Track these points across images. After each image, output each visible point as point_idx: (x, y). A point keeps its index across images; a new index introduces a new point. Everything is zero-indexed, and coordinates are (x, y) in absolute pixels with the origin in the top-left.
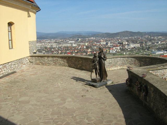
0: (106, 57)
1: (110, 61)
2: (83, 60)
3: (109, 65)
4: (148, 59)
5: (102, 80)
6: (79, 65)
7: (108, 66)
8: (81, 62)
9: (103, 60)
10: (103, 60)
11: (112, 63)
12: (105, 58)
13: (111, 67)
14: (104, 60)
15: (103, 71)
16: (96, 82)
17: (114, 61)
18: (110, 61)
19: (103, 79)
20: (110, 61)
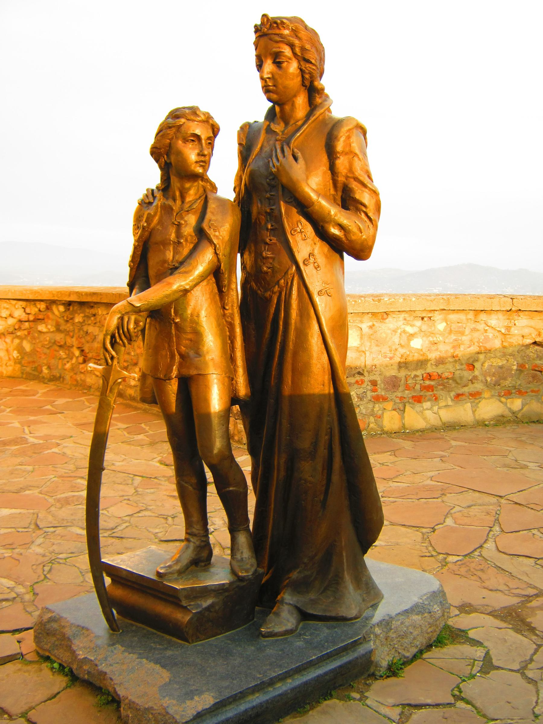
9: (305, 244)
10: (305, 244)
12: (347, 200)
13: (418, 399)
15: (305, 443)
17: (453, 337)
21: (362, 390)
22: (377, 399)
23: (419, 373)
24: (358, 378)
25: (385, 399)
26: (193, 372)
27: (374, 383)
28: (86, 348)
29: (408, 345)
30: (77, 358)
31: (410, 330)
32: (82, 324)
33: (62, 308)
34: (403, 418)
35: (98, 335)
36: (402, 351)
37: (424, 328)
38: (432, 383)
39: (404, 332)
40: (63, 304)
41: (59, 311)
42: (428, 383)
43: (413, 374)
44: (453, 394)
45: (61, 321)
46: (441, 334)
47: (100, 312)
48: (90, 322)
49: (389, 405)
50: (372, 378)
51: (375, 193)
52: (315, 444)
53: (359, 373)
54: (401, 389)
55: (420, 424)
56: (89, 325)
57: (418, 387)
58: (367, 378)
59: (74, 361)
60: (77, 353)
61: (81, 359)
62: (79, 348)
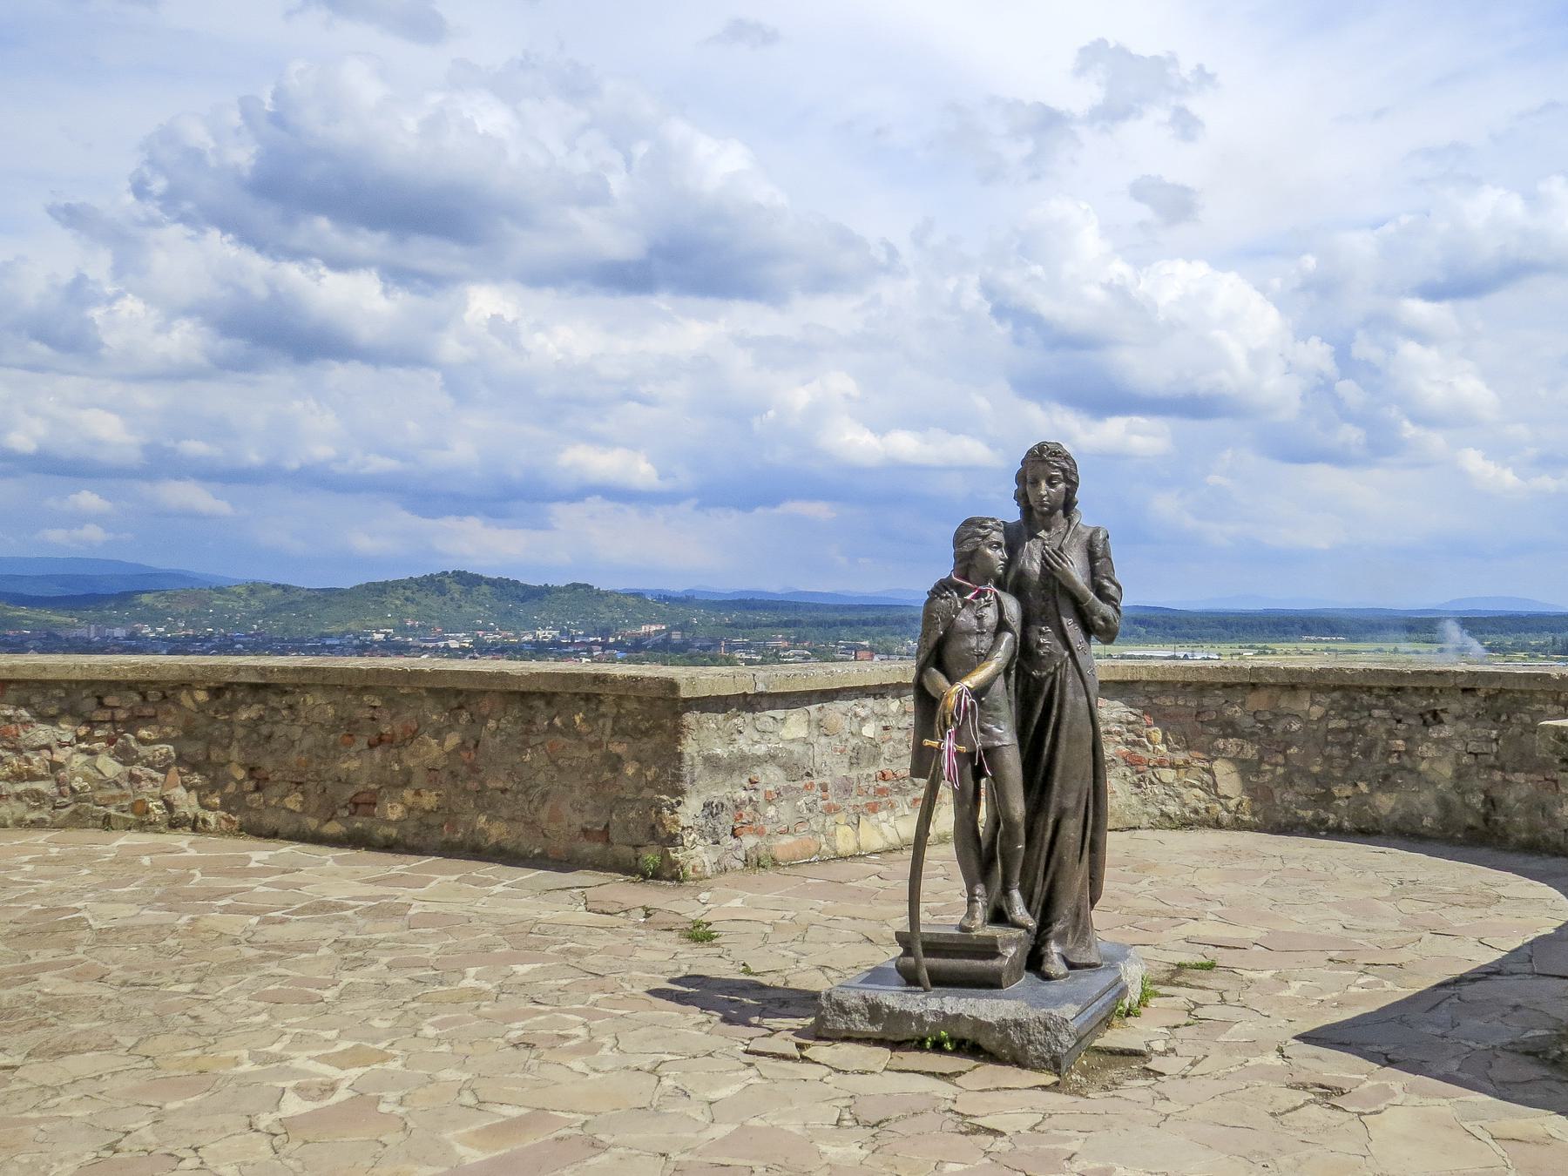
0: (1112, 590)
1: (864, 719)
2: (478, 720)
3: (854, 774)
4: (1312, 708)
5: (1054, 949)
6: (408, 794)
7: (846, 788)
8: (452, 740)
11: (886, 750)
13: (874, 809)
14: (1088, 629)
16: (989, 983)
18: (869, 730)
19: (1057, 927)
20: (869, 730)
21: (811, 798)
22: (830, 810)
23: (872, 771)
24: (807, 781)
25: (837, 810)
26: (997, 743)
27: (824, 788)
28: (268, 764)
29: (860, 734)
30: (240, 783)
31: (862, 713)
32: (253, 725)
33: (201, 696)
34: (858, 834)
35: (300, 740)
36: (854, 741)
37: (877, 709)
38: (886, 785)
39: (856, 715)
40: (209, 690)
41: (195, 701)
42: (882, 784)
43: (866, 771)
44: (909, 799)
45: (201, 720)
46: (895, 716)
47: (310, 700)
48: (278, 718)
49: (841, 818)
50: (821, 780)
51: (1120, 588)
52: (1079, 802)
53: (808, 774)
54: (854, 793)
55: (878, 844)
56: (276, 723)
57: (871, 791)
58: (817, 781)
59: (231, 788)
60: (240, 774)
61: (251, 785)
62: (242, 766)
